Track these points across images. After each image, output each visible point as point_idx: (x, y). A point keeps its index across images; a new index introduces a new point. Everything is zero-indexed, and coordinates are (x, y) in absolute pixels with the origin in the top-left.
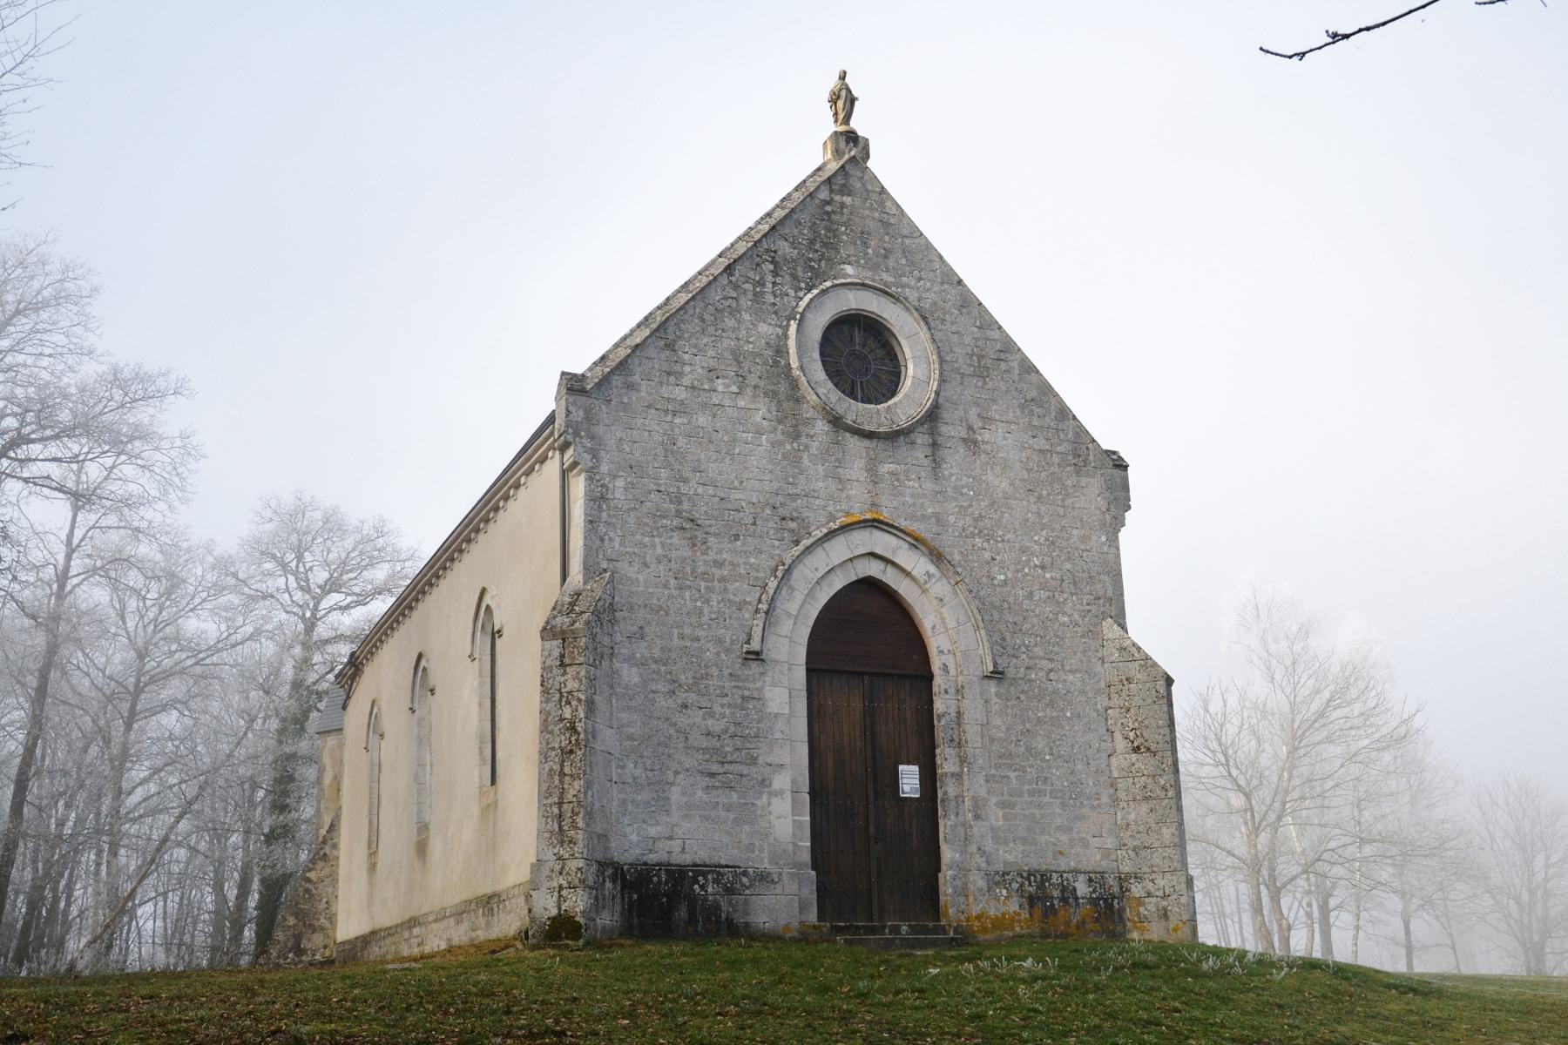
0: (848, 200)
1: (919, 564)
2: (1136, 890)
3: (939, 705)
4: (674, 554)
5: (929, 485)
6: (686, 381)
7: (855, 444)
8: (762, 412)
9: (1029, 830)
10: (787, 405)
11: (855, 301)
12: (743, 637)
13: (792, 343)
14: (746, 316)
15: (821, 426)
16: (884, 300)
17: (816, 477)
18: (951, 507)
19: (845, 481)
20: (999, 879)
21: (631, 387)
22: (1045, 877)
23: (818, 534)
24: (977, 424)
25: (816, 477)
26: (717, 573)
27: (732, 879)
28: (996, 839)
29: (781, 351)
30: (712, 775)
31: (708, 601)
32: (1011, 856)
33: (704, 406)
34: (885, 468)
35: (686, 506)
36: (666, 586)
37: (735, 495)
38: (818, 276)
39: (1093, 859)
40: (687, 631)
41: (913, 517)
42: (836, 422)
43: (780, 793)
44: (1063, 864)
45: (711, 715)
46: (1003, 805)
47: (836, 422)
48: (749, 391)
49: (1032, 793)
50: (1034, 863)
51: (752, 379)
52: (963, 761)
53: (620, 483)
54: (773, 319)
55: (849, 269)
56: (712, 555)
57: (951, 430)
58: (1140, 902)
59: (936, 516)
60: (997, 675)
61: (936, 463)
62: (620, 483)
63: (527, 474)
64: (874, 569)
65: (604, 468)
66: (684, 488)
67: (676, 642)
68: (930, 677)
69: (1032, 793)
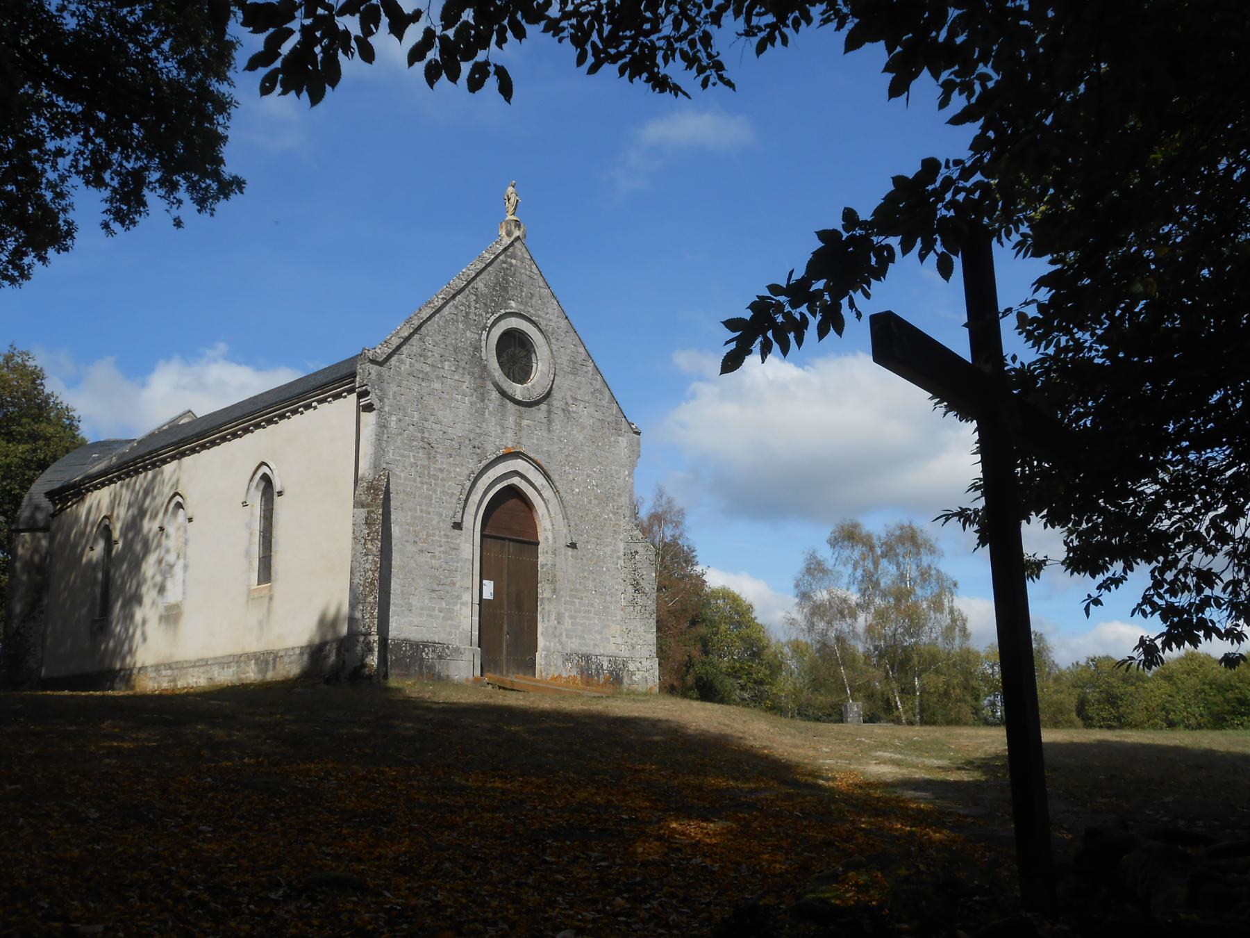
0: (514, 261)
1: (539, 480)
2: (632, 667)
3: (541, 560)
4: (419, 463)
5: (545, 434)
6: (429, 361)
7: (510, 405)
8: (467, 384)
9: (583, 631)
10: (479, 381)
11: (514, 323)
12: (451, 513)
13: (483, 343)
14: (461, 326)
15: (495, 395)
16: (535, 329)
17: (492, 426)
18: (555, 448)
19: (501, 431)
20: (567, 658)
21: (402, 362)
22: (588, 658)
23: (493, 457)
24: (571, 401)
25: (492, 426)
26: (440, 475)
27: (443, 651)
28: (567, 636)
29: (477, 349)
30: (434, 591)
31: (435, 491)
32: (573, 645)
33: (438, 378)
34: (525, 423)
35: (426, 435)
36: (415, 481)
37: (450, 431)
38: (498, 306)
39: (612, 649)
40: (424, 508)
41: (537, 452)
42: (503, 393)
43: (464, 604)
44: (597, 652)
45: (434, 557)
46: (571, 617)
47: (503, 393)
48: (461, 371)
49: (586, 611)
50: (584, 650)
51: (462, 364)
52: (554, 591)
53: (394, 418)
54: (473, 329)
55: (513, 304)
56: (439, 466)
57: (557, 401)
58: (633, 674)
59: (548, 452)
60: (573, 546)
61: (550, 422)
62: (394, 418)
63: (320, 402)
64: (516, 480)
65: (387, 409)
66: (426, 424)
67: (418, 513)
68: (538, 544)
69: (586, 611)
